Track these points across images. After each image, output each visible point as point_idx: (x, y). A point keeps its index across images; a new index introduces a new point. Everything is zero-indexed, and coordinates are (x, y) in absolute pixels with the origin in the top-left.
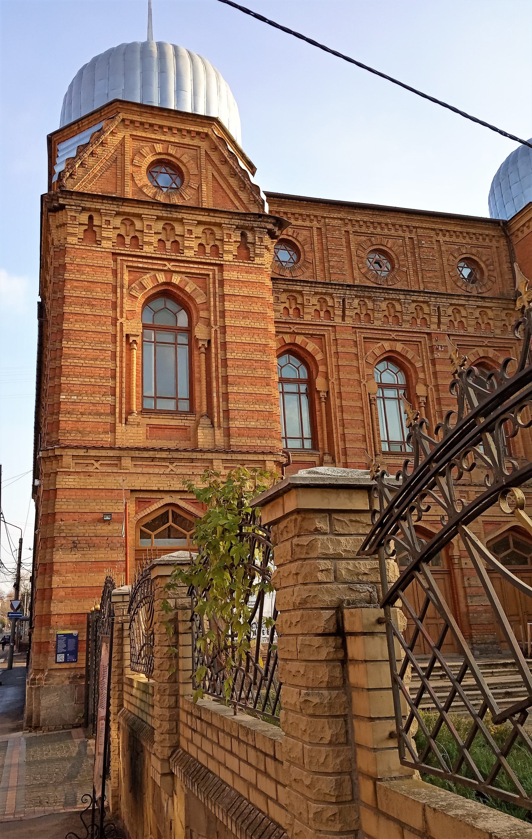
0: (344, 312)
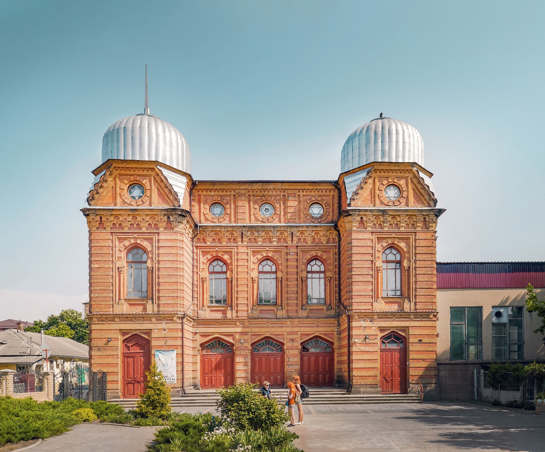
0: (242, 238)
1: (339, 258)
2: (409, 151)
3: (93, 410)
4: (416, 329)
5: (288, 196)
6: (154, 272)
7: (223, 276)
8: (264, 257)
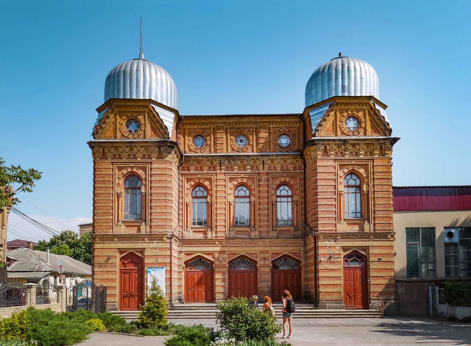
1: (305, 184)
2: (366, 86)
3: (102, 321)
4: (375, 248)
5: (260, 129)
6: (147, 196)
7: (204, 200)
8: (239, 183)
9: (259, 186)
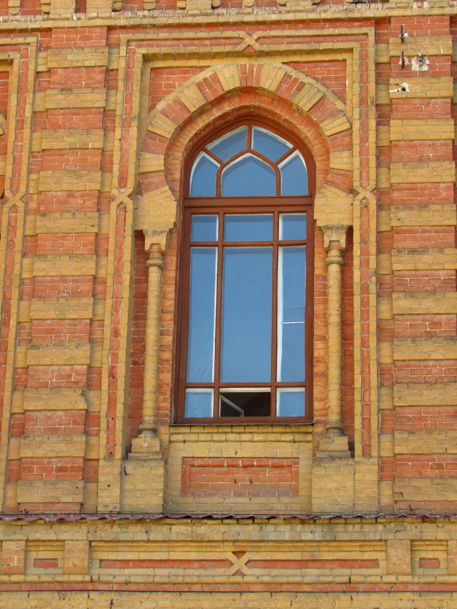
9: (384, 114)
